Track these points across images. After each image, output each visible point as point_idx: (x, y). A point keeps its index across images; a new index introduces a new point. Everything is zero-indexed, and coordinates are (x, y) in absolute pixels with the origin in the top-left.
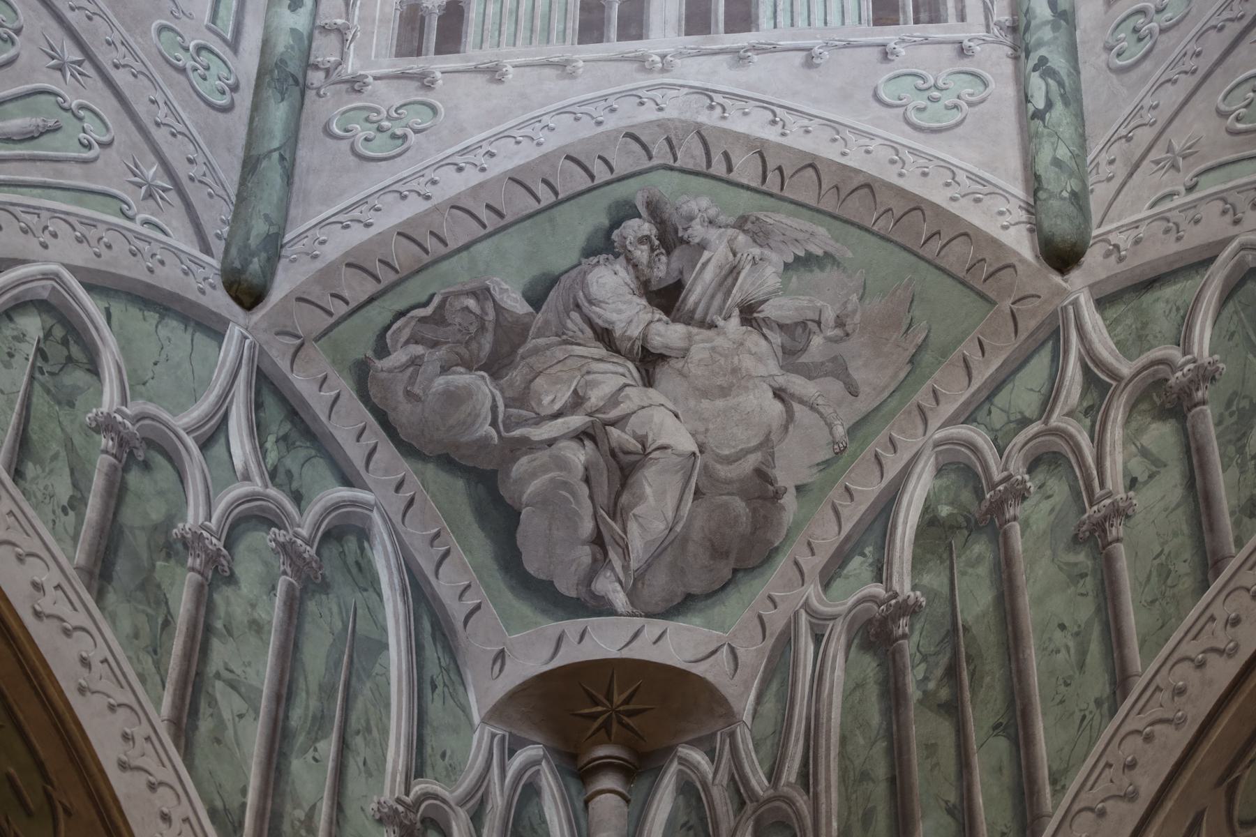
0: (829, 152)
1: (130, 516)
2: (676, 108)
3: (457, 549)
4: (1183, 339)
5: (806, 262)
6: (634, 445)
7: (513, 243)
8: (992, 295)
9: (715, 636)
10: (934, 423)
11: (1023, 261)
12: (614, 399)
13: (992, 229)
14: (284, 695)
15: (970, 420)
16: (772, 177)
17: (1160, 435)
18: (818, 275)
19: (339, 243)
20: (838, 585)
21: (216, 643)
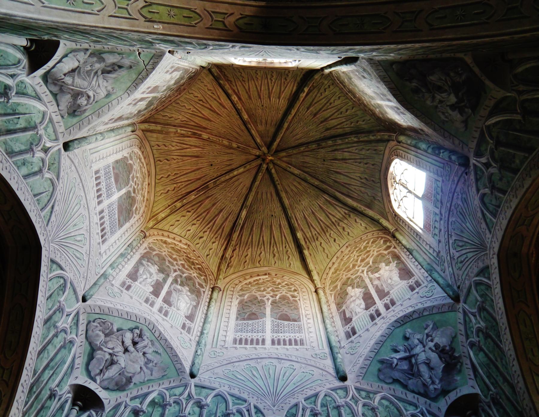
0: (170, 340)
1: (54, 317)
2: (153, 319)
3: (82, 357)
4: (206, 398)
5: (157, 352)
6: (116, 361)
7: (121, 320)
9: (108, 397)
10: (160, 387)
12: (118, 352)
13: (185, 366)
14: (52, 360)
15: (167, 390)
16: (160, 338)
17: (197, 410)
18: (157, 355)
19: (99, 303)
20: (133, 401)
21: (50, 344)
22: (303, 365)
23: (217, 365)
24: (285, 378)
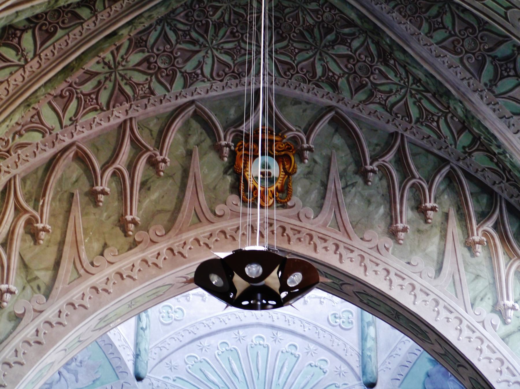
8: (120, 377)
11: (130, 373)
22: (312, 346)
23: (175, 344)
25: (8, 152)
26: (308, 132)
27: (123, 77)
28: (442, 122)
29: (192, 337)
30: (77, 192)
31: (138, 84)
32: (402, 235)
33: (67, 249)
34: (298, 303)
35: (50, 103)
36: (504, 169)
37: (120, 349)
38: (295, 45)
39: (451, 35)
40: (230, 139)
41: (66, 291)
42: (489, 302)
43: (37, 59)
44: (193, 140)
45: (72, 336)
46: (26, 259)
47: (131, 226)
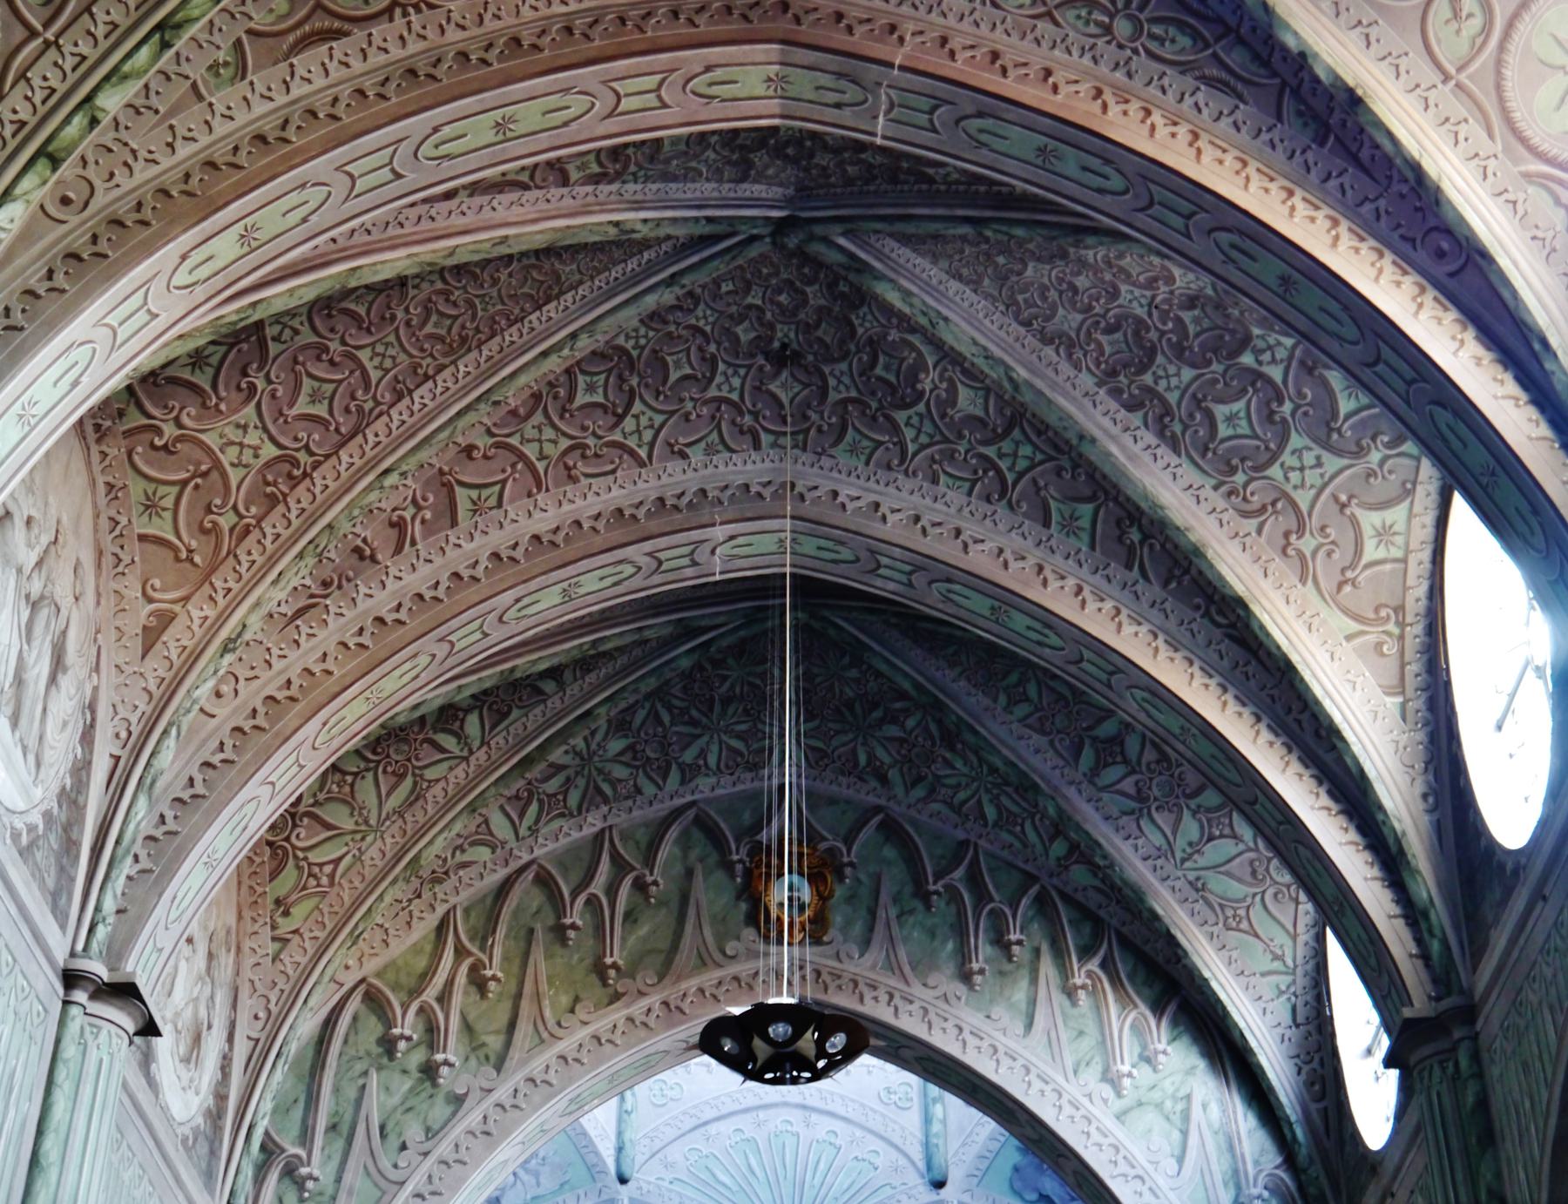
22: (859, 1133)
23: (671, 1133)
24: (817, 1181)
25: (446, 873)
26: (849, 841)
27: (600, 771)
28: (1028, 825)
29: (695, 1122)
30: (538, 927)
31: (620, 781)
32: (978, 979)
33: (525, 1005)
34: (840, 1076)
35: (502, 808)
36: (1113, 886)
37: (597, 1141)
38: (830, 725)
39: (1037, 710)
40: (744, 851)
41: (523, 1063)
42: (1097, 1068)
43: (485, 749)
44: (694, 854)
45: (531, 1124)
46: (470, 1018)
47: (612, 973)
